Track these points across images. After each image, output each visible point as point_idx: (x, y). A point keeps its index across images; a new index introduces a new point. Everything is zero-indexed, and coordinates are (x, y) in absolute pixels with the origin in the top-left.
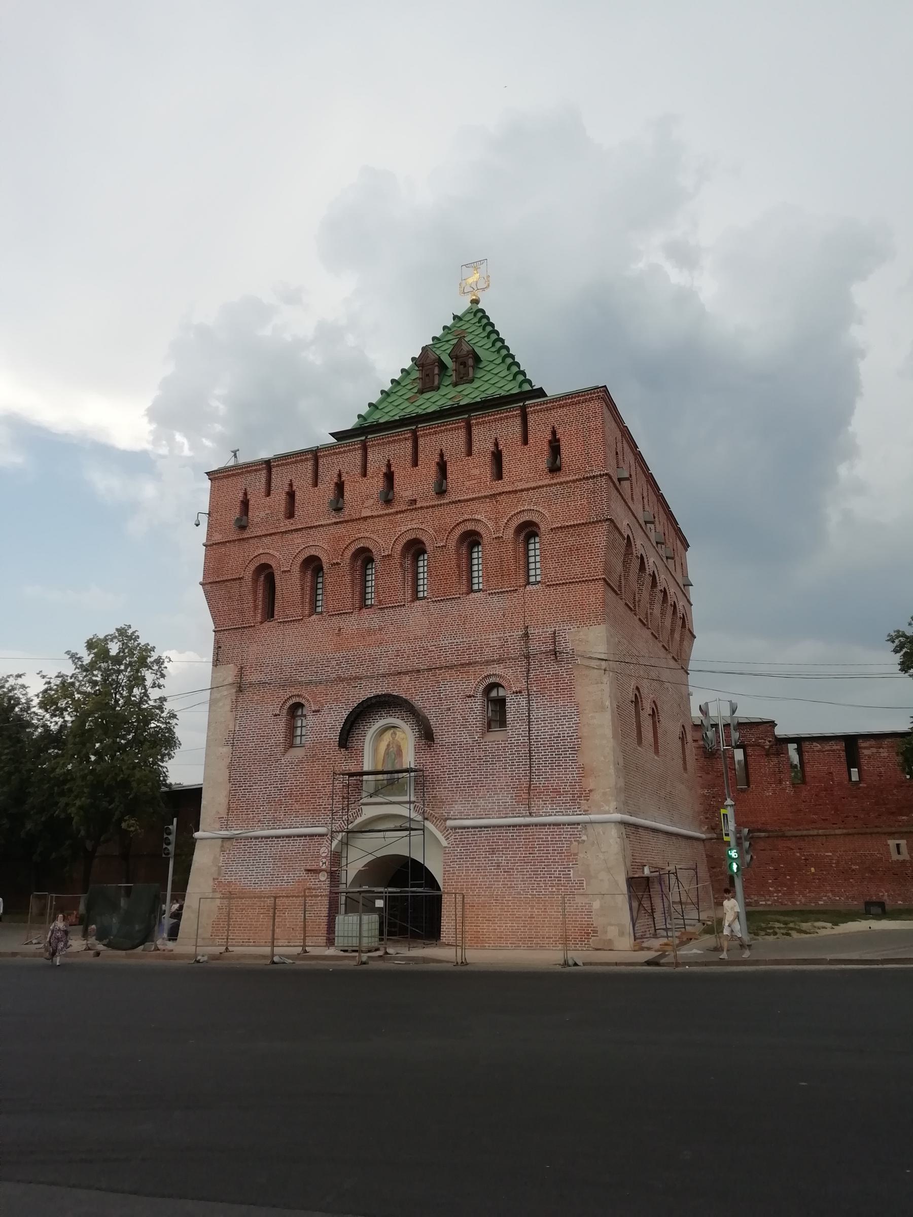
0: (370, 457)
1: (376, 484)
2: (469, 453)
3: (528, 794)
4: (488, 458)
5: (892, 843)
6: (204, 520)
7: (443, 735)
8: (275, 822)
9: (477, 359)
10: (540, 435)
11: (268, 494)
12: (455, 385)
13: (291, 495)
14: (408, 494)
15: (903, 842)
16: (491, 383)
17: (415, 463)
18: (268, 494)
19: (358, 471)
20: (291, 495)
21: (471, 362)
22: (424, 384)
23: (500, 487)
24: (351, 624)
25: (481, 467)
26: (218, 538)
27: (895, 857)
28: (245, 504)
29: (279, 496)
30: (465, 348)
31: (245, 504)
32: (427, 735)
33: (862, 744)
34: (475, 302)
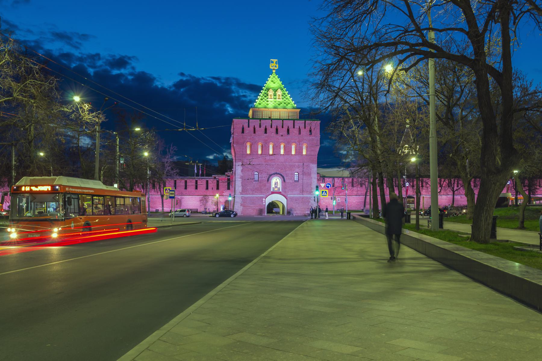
1: (274, 130)
2: (294, 127)
3: (302, 192)
7: (287, 181)
8: (253, 194)
10: (308, 128)
11: (249, 127)
13: (254, 129)
14: (281, 134)
17: (283, 127)
18: (249, 127)
20: (254, 129)
24: (268, 158)
25: (296, 131)
29: (252, 128)
32: (284, 181)
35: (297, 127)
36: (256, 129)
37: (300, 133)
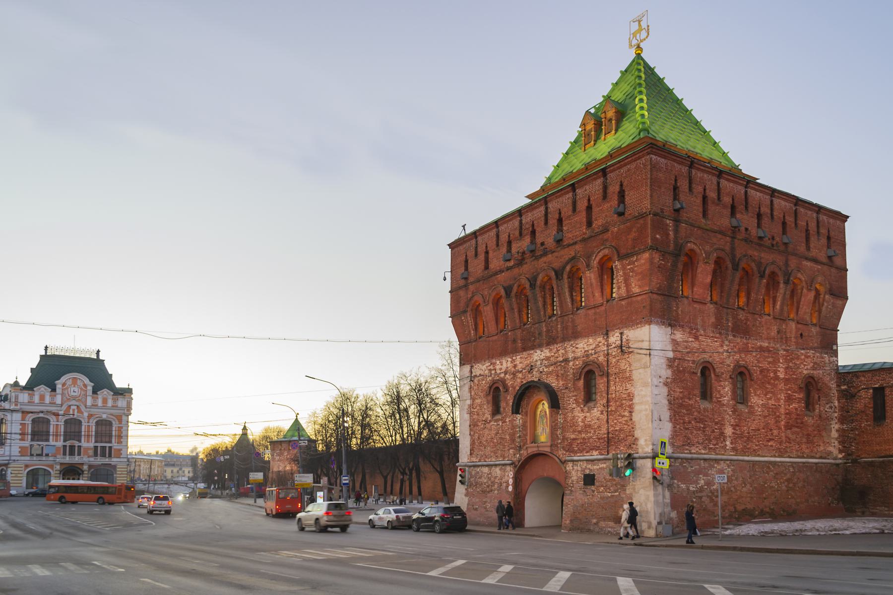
6: (448, 276)
19: (517, 233)
36: (491, 255)
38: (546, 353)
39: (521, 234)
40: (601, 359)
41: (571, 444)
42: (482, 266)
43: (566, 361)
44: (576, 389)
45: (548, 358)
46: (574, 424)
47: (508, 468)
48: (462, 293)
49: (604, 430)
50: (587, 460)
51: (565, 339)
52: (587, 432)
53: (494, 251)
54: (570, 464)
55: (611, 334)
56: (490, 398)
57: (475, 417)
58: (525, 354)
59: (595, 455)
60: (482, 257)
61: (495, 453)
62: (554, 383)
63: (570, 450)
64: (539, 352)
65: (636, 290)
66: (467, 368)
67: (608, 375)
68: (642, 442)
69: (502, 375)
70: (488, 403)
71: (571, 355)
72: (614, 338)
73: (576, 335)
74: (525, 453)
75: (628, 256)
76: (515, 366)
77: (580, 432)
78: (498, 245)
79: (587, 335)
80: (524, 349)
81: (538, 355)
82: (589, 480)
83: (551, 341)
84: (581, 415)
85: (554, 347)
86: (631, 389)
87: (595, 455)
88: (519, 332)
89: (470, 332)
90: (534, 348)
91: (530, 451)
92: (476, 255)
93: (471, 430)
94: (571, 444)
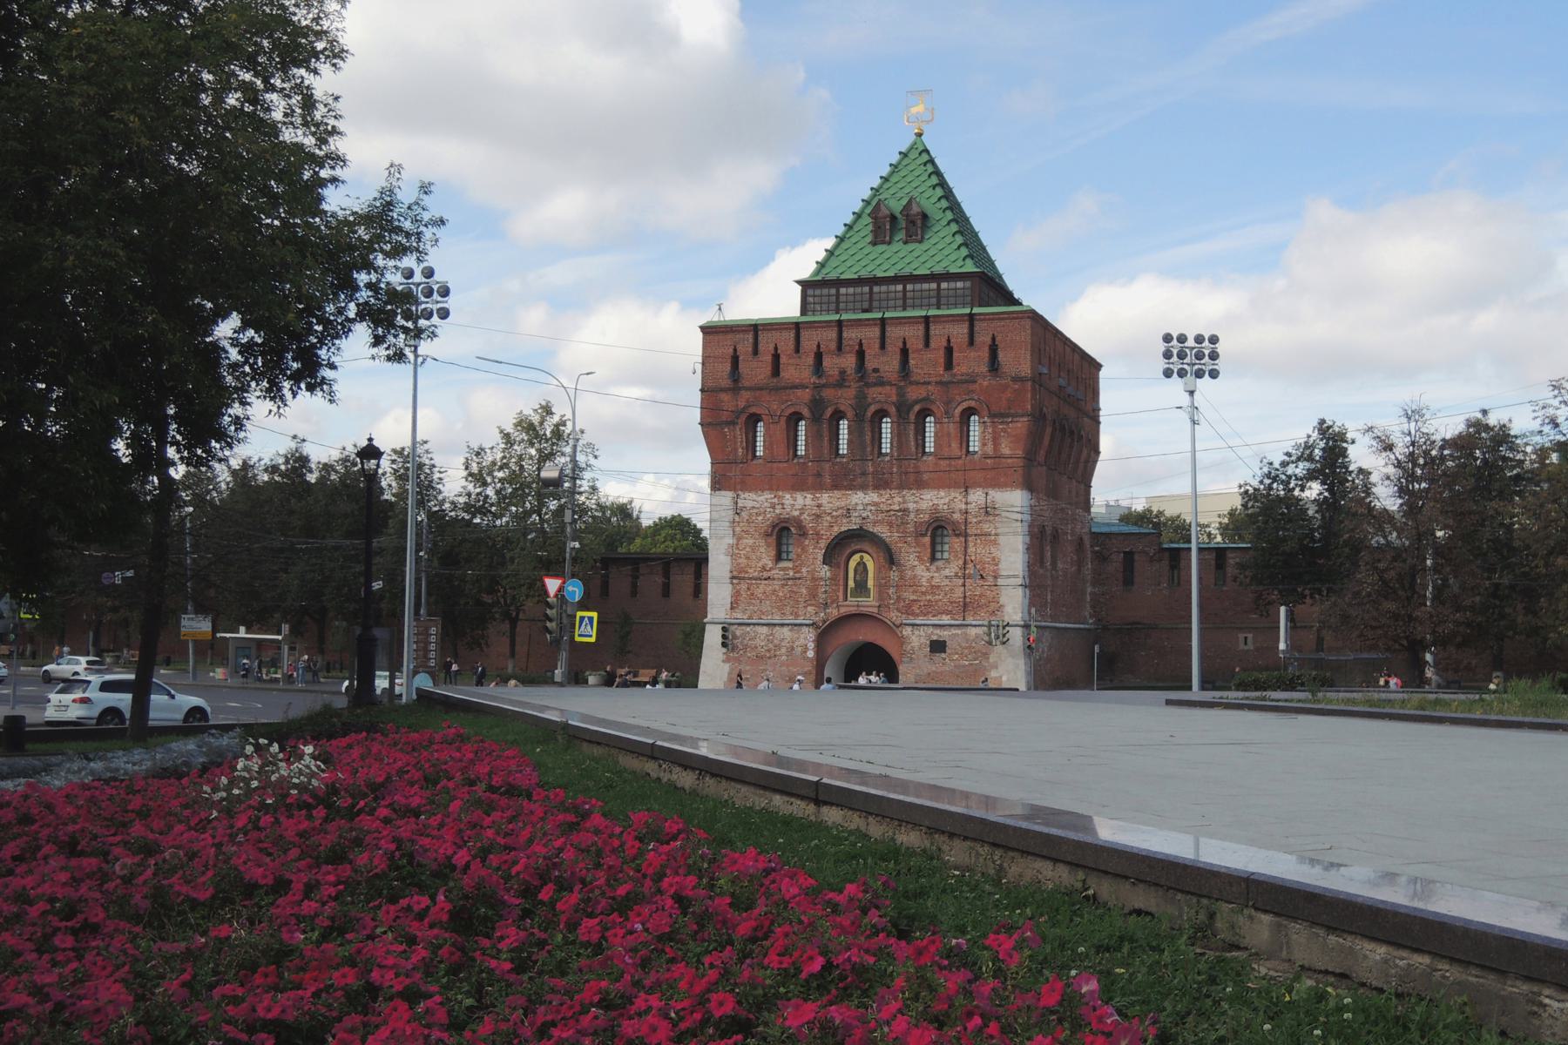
0: (845, 335)
4: (942, 352)
5: (1241, 636)
6: (699, 368)
9: (925, 216)
12: (906, 243)
15: (1250, 636)
16: (937, 253)
19: (833, 346)
21: (919, 223)
22: (876, 237)
23: (946, 378)
26: (710, 384)
27: (1242, 646)
28: (735, 360)
30: (915, 209)
31: (735, 360)
33: (1230, 555)
34: (919, 135)
35: (938, 342)
36: (783, 360)
37: (949, 365)
38: (873, 497)
39: (839, 348)
40: (957, 516)
41: (909, 606)
42: (768, 370)
43: (905, 511)
44: (918, 544)
45: (876, 504)
46: (914, 584)
47: (805, 629)
48: (725, 397)
49: (959, 592)
50: (934, 626)
51: (901, 487)
52: (934, 594)
53: (790, 357)
54: (909, 629)
55: (971, 491)
56: (773, 540)
57: (743, 561)
58: (837, 493)
59: (946, 620)
60: (769, 358)
61: (780, 609)
62: (882, 531)
63: (908, 610)
64: (860, 494)
65: (1006, 451)
66: (726, 498)
67: (966, 536)
68: (1009, 609)
69: (796, 513)
70: (768, 545)
71: (911, 506)
72: (977, 497)
73: (920, 485)
74: (834, 613)
75: (1002, 415)
76: (819, 506)
77: (923, 593)
78: (797, 351)
79: (939, 487)
80: (836, 486)
81: (858, 498)
82: (938, 647)
83: (881, 484)
84: (927, 574)
85: (886, 494)
86: (996, 553)
87: (946, 620)
88: (827, 466)
89: (736, 450)
90: (852, 487)
91: (843, 610)
92: (756, 352)
93: (733, 578)
94: (909, 606)
